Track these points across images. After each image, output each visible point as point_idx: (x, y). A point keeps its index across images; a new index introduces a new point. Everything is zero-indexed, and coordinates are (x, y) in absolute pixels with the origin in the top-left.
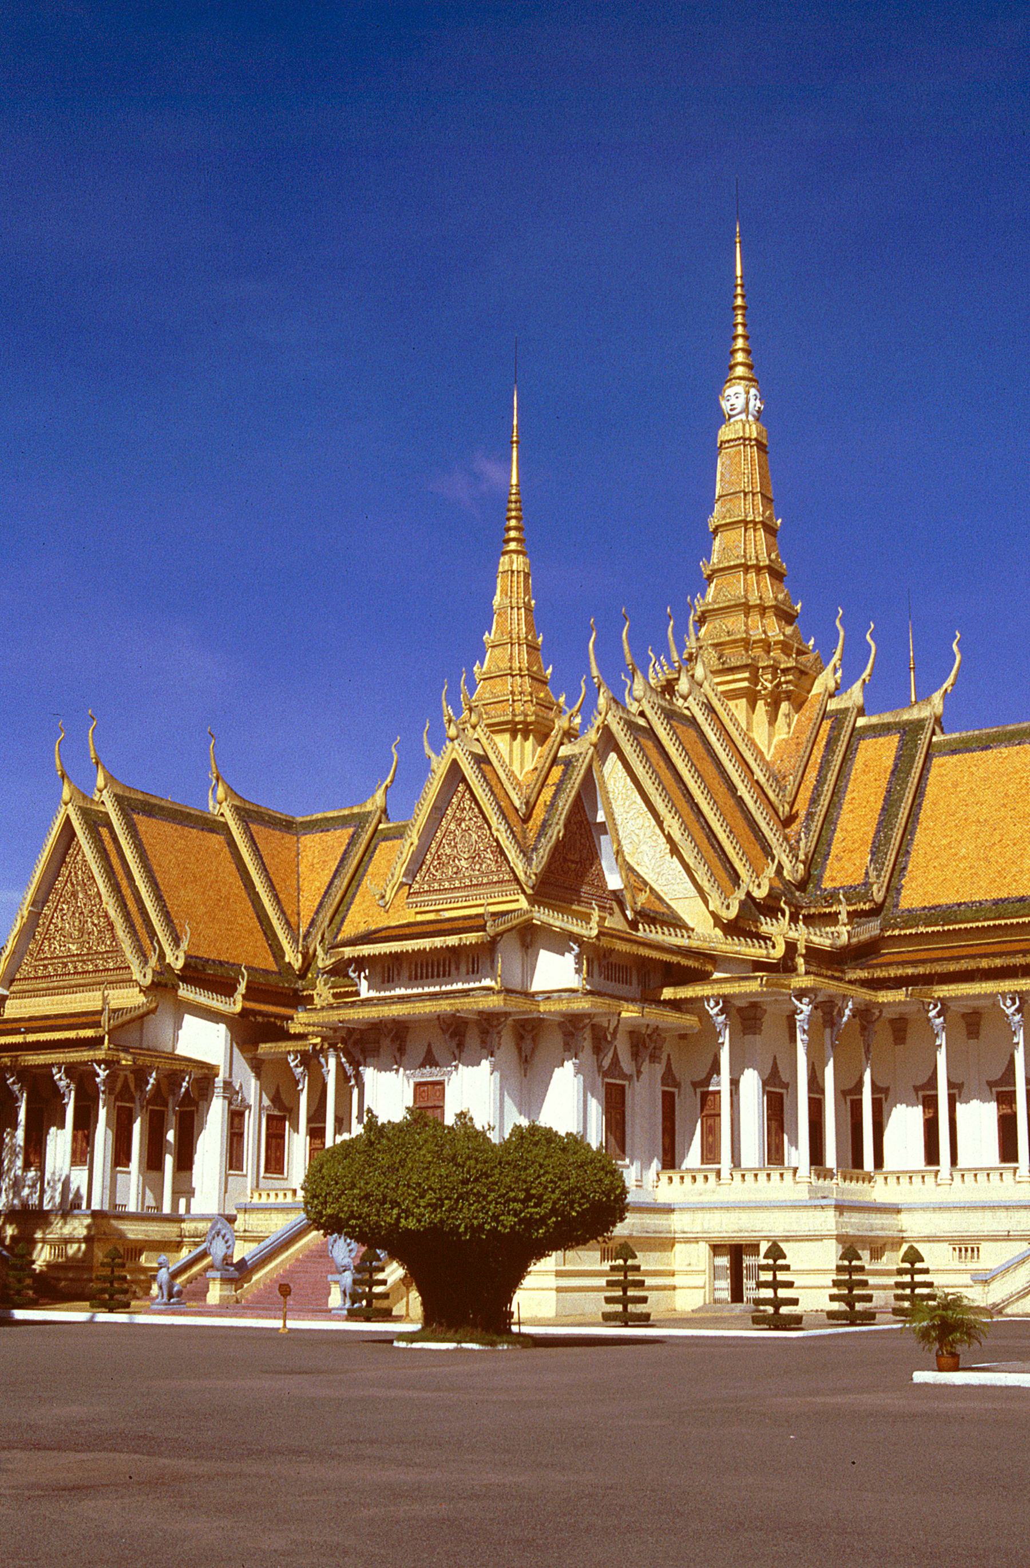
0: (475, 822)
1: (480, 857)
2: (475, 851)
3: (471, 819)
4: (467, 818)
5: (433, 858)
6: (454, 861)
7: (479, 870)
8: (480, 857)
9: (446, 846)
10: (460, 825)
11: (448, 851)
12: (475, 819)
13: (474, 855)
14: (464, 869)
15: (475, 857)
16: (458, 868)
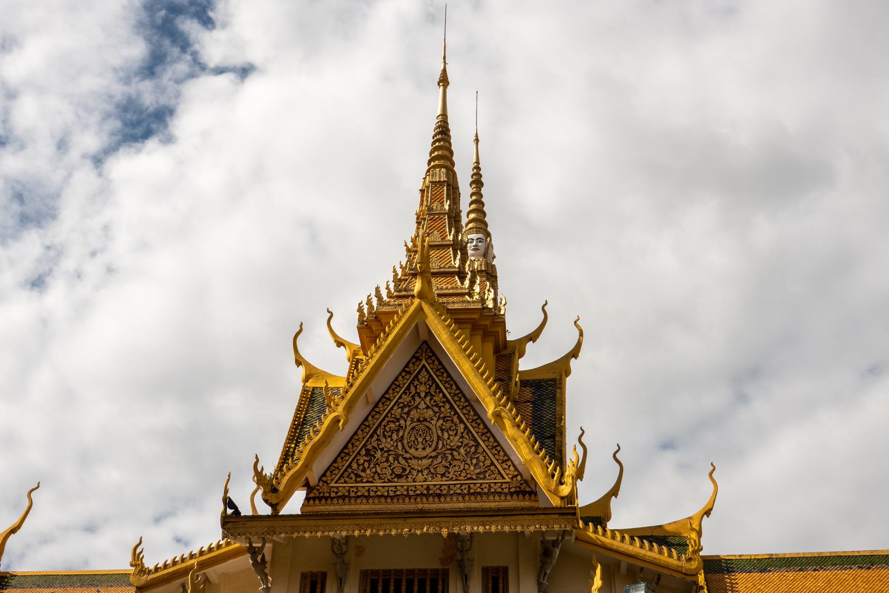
0: (436, 413)
1: (445, 457)
2: (434, 450)
3: (428, 407)
4: (422, 406)
5: (359, 453)
6: (396, 458)
7: (443, 475)
8: (445, 457)
9: (384, 440)
10: (408, 413)
11: (386, 444)
12: (436, 409)
13: (434, 454)
14: (415, 473)
15: (436, 457)
16: (404, 470)
